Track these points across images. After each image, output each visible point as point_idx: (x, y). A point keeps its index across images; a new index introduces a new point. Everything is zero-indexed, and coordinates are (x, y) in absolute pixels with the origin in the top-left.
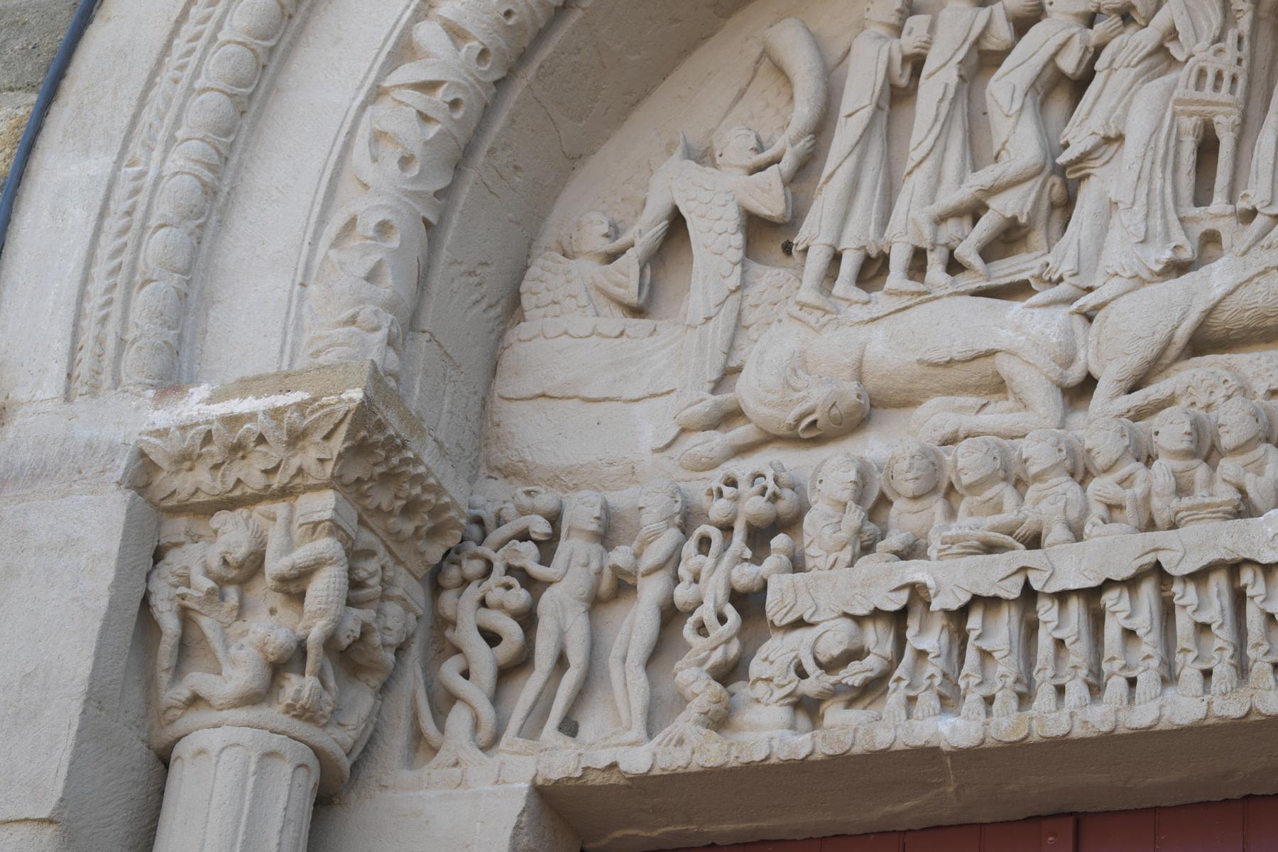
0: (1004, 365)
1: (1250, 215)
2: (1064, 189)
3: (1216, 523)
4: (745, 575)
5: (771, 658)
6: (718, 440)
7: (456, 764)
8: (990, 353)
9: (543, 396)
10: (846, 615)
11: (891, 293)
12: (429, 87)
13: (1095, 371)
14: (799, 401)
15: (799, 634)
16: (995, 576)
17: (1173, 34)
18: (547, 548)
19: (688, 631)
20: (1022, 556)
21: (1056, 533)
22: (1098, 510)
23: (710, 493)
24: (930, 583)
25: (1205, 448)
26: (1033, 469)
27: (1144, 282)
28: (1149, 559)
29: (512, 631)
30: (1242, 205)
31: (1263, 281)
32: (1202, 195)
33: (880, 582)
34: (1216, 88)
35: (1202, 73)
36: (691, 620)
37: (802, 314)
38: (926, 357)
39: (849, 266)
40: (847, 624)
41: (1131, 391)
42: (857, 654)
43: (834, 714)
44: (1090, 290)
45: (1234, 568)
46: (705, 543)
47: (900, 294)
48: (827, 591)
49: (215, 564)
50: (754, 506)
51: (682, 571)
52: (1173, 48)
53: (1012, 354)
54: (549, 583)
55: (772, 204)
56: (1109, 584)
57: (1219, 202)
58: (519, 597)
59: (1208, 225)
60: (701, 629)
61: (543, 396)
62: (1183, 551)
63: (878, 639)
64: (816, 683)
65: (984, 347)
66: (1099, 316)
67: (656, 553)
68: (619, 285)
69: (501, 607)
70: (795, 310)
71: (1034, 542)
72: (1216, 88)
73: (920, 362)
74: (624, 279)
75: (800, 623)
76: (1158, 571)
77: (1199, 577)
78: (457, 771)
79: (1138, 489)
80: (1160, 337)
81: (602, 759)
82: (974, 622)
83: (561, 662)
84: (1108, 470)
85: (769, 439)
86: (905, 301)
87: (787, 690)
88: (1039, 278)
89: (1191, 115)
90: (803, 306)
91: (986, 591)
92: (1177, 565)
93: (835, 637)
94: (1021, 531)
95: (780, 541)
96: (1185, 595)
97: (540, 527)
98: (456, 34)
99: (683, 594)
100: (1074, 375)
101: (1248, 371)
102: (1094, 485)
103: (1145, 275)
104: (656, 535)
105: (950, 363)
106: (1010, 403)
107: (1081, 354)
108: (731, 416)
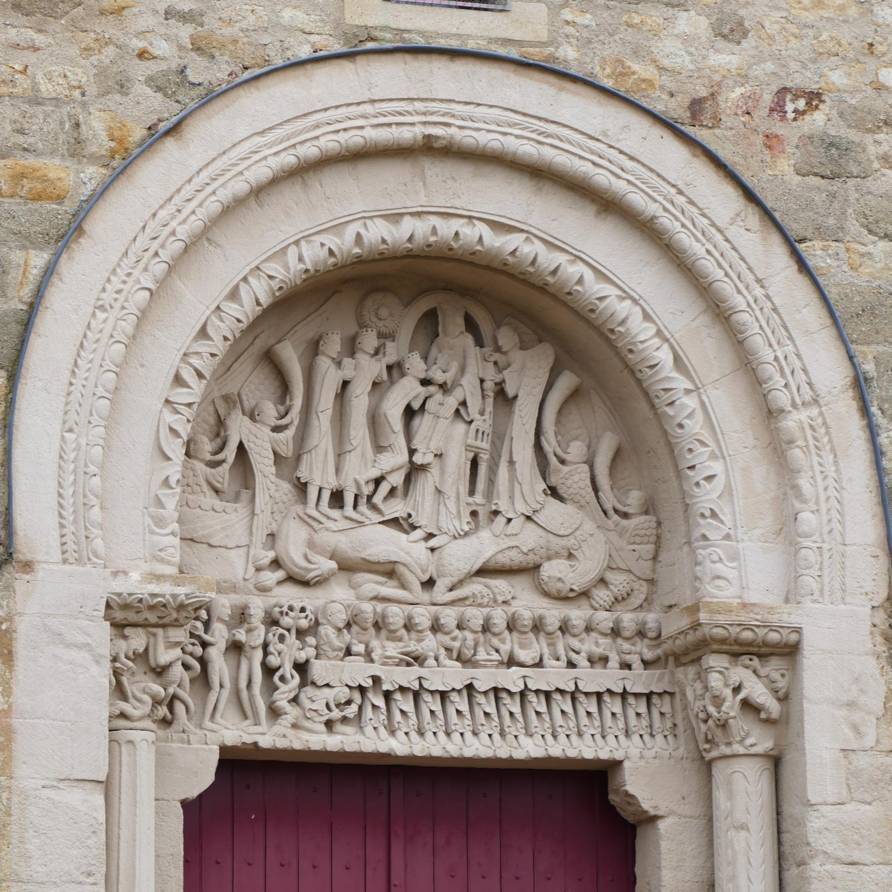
0: (401, 569)
1: (496, 513)
2: (414, 471)
3: (493, 670)
4: (302, 656)
5: (314, 698)
6: (271, 577)
7: (184, 732)
8: (395, 562)
9: (192, 540)
10: (347, 685)
11: (347, 518)
12: (189, 405)
13: (435, 576)
14: (315, 569)
15: (326, 690)
16: (408, 676)
17: (464, 403)
18: (207, 624)
19: (276, 678)
20: (416, 670)
21: (431, 662)
22: (442, 651)
23: (281, 613)
24: (383, 677)
25: (486, 628)
26: (420, 628)
27: (455, 538)
28: (468, 682)
29: (197, 665)
30: (494, 508)
31: (507, 552)
32: (472, 492)
33: (358, 671)
34: (482, 441)
35: (477, 431)
36: (278, 674)
37: (310, 521)
38: (367, 558)
39: (326, 495)
40: (347, 690)
41: (451, 590)
42: (349, 702)
43: (339, 727)
44: (431, 536)
45: (496, 690)
46: (282, 638)
47: (352, 520)
48: (338, 674)
49: (131, 654)
50: (304, 623)
51: (271, 648)
52: (462, 411)
53: (404, 565)
54: (211, 644)
55: (287, 450)
56: (453, 689)
57: (478, 498)
58: (199, 650)
59: (474, 508)
60: (282, 679)
61: (192, 540)
62: (484, 679)
63: (357, 697)
64: (336, 714)
65: (394, 559)
66: (437, 552)
67: (258, 637)
68: (219, 482)
69: (191, 654)
70: (306, 518)
71: (418, 659)
72: (482, 441)
73: (363, 559)
74: (221, 480)
75: (327, 685)
76: (470, 687)
77: (485, 693)
78: (185, 736)
79: (457, 644)
80: (466, 571)
81: (249, 740)
82: (398, 696)
83: (221, 686)
84: (446, 634)
85: (292, 579)
86: (354, 525)
87: (326, 718)
88: (406, 520)
89: (471, 451)
90: (309, 517)
91: (405, 684)
92: (481, 686)
93: (343, 694)
94: (413, 655)
95: (311, 640)
96: (481, 699)
97: (203, 614)
98: (200, 375)
99: (273, 661)
100: (425, 578)
101: (496, 591)
102: (439, 636)
103: (457, 536)
104: (256, 628)
105: (379, 562)
106: (394, 583)
107: (430, 569)
108: (276, 564)
